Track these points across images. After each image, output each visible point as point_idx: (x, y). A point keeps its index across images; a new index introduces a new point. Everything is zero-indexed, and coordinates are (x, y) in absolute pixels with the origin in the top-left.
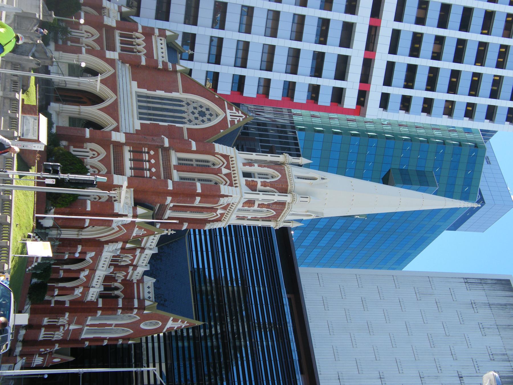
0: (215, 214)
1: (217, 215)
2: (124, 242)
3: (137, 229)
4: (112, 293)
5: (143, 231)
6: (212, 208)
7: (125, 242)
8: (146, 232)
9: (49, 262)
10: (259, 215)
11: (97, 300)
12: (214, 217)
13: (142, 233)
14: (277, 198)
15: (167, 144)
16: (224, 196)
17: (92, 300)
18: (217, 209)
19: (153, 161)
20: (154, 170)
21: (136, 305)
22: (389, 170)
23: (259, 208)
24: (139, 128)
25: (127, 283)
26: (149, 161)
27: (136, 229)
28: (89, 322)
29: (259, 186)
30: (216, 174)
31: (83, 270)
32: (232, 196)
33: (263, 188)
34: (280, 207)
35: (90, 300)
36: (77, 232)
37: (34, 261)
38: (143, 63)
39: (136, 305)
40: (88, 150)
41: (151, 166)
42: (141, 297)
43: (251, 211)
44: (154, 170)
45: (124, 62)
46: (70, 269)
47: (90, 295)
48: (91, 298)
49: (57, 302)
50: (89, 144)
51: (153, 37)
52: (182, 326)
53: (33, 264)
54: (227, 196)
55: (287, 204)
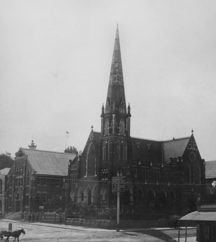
0: (125, 143)
1: (125, 142)
12: (126, 143)
19: (105, 170)
20: (107, 170)
23: (120, 126)
24: (96, 175)
26: (105, 171)
28: (190, 184)
29: (111, 128)
30: (108, 145)
33: (111, 126)
40: (103, 194)
41: (106, 171)
44: (107, 170)
50: (101, 193)
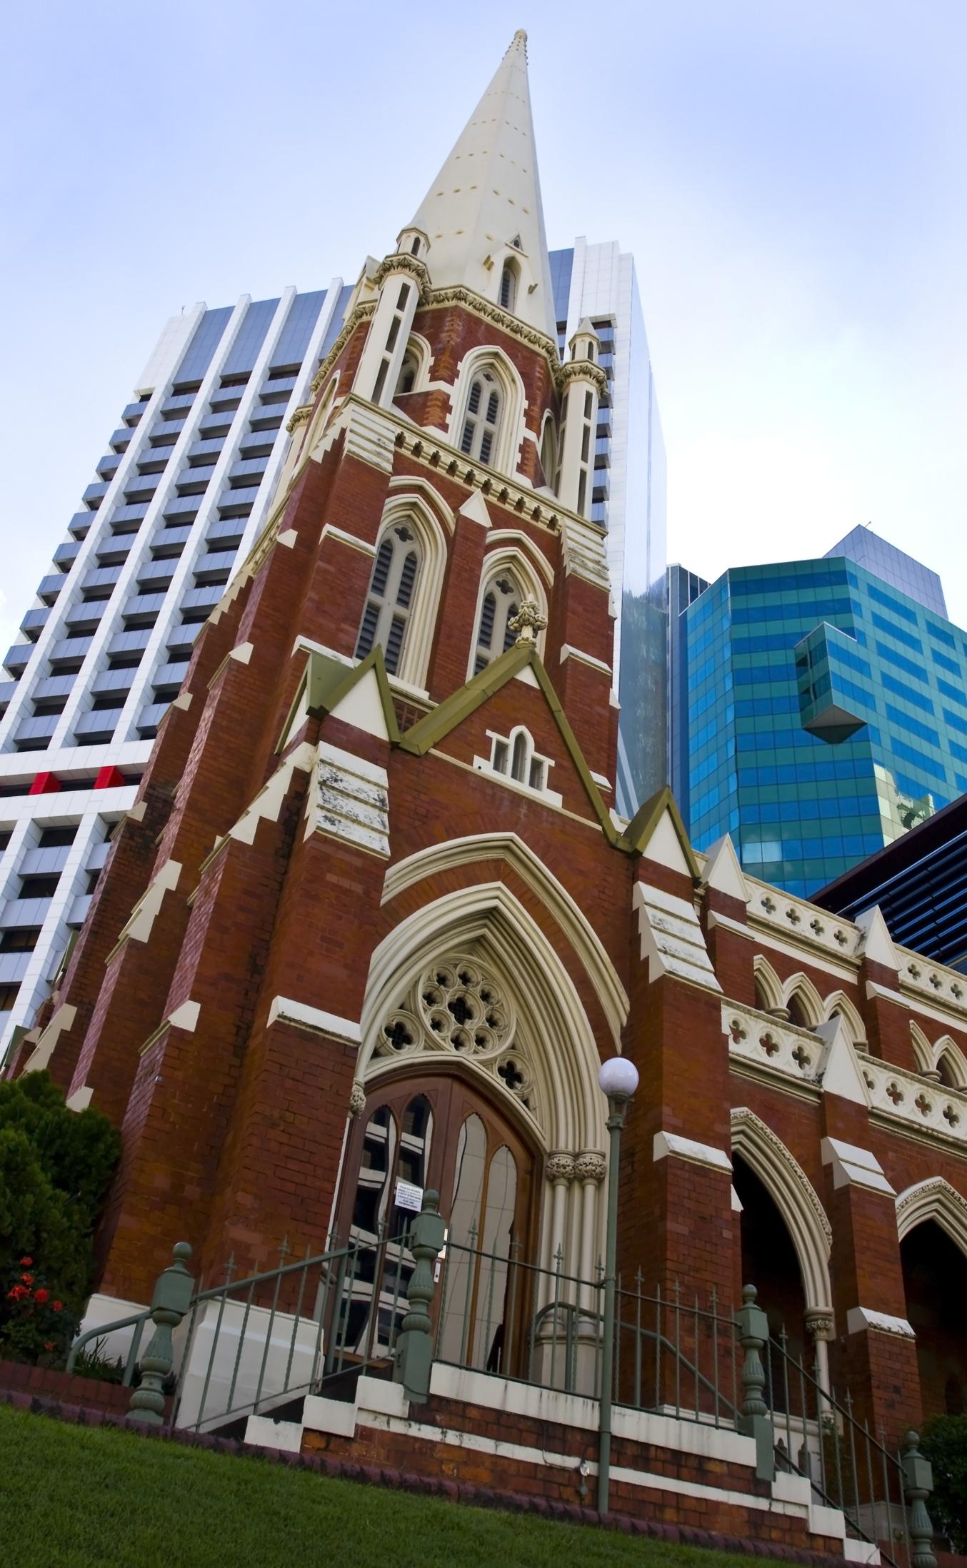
2: (634, 879)
5: (511, 742)
6: (451, 542)
9: (755, 1357)
13: (531, 751)
18: (462, 521)
22: (807, 729)
27: (483, 767)
36: (561, 1190)
37: (762, 1504)
53: (799, 1525)
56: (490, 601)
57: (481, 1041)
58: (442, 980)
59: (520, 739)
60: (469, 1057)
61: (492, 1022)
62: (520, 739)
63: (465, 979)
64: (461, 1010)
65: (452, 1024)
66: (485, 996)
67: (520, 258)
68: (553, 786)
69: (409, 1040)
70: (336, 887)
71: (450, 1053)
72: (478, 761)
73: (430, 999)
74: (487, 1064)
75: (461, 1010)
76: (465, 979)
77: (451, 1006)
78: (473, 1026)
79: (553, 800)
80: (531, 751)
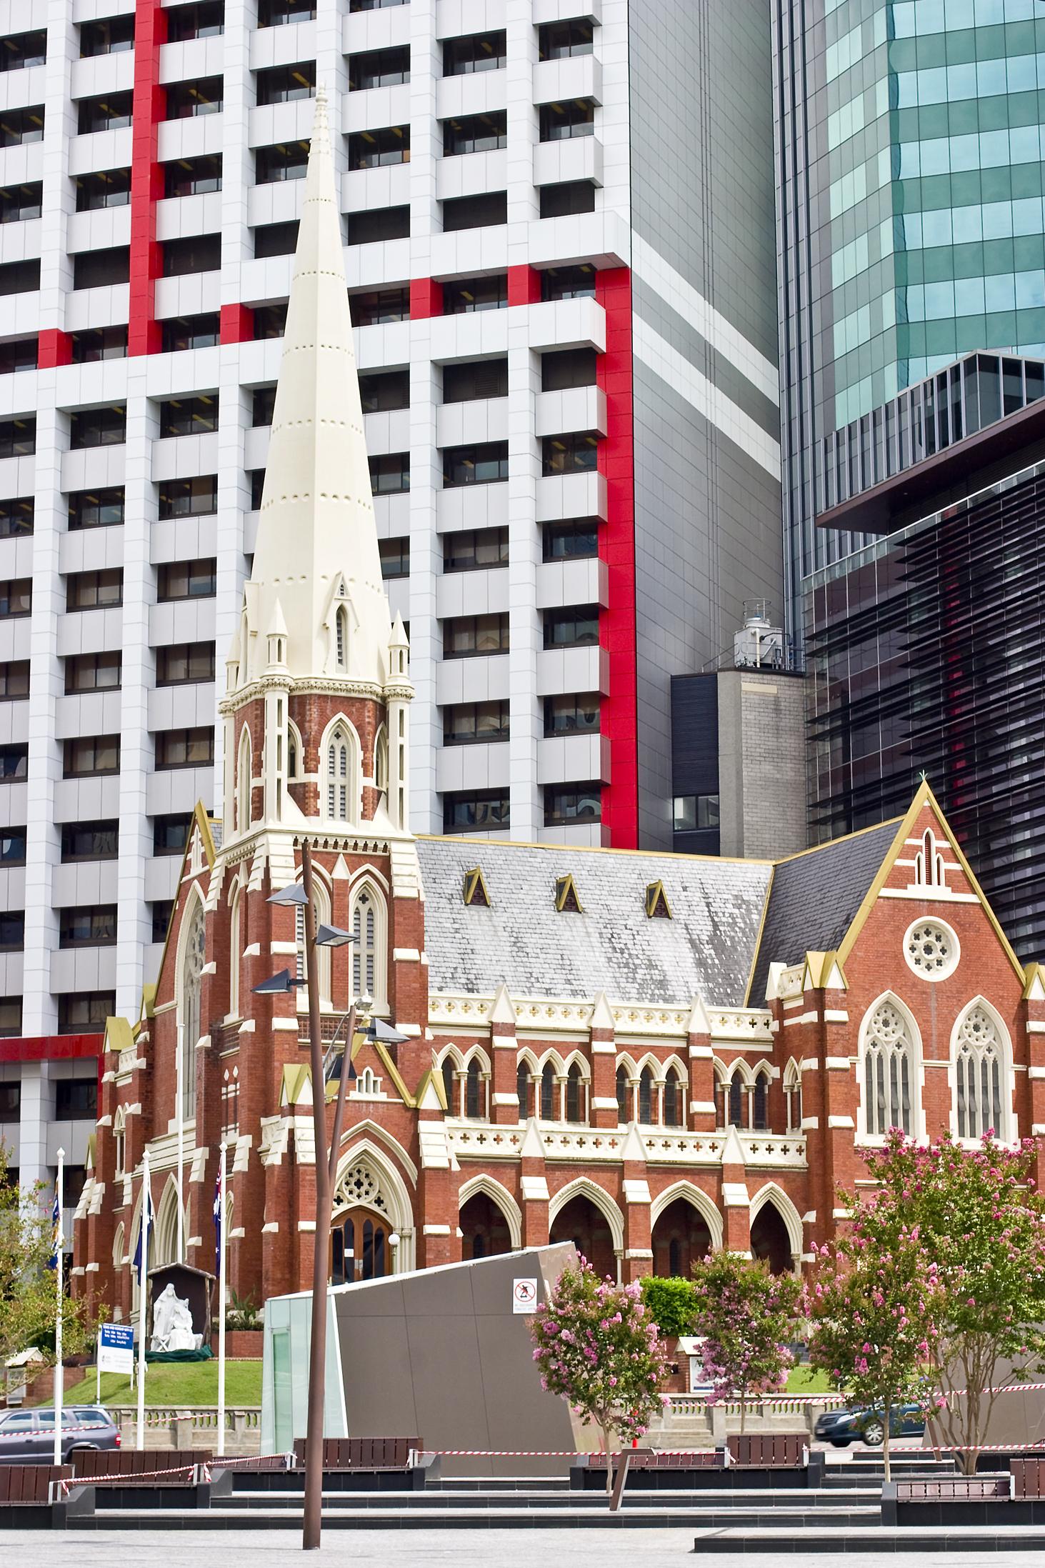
1: (368, 872)
3: (351, 1092)
4: (792, 1093)
5: (364, 1078)
6: (331, 895)
7: (416, 1114)
8: (368, 1068)
10: (357, 755)
11: (805, 1132)
14: (278, 726)
15: (205, 1041)
16: (267, 881)
17: (804, 1147)
21: (812, 1017)
25: (782, 1048)
31: (621, 1198)
32: (268, 857)
34: (310, 710)
35: (804, 1154)
38: (135, 1108)
39: (812, 1017)
42: (800, 1002)
43: (338, 780)
45: (138, 1159)
46: (624, 1232)
47: (777, 1159)
48: (793, 1152)
49: (807, 1249)
51: (119, 1085)
52: (939, 850)
54: (267, 871)
55: (295, 693)
56: (357, 912)
57: (367, 1193)
58: (351, 1175)
59: (368, 1073)
60: (363, 1202)
61: (370, 1184)
62: (368, 1073)
63: (359, 1171)
64: (359, 1184)
65: (356, 1191)
66: (367, 1176)
67: (347, 605)
68: (382, 1091)
69: (342, 1201)
70: (311, 1180)
71: (357, 1203)
72: (352, 1093)
73: (347, 1184)
74: (370, 1203)
75: (359, 1184)
76: (359, 1171)
77: (355, 1184)
78: (363, 1189)
79: (382, 1097)
80: (372, 1078)
